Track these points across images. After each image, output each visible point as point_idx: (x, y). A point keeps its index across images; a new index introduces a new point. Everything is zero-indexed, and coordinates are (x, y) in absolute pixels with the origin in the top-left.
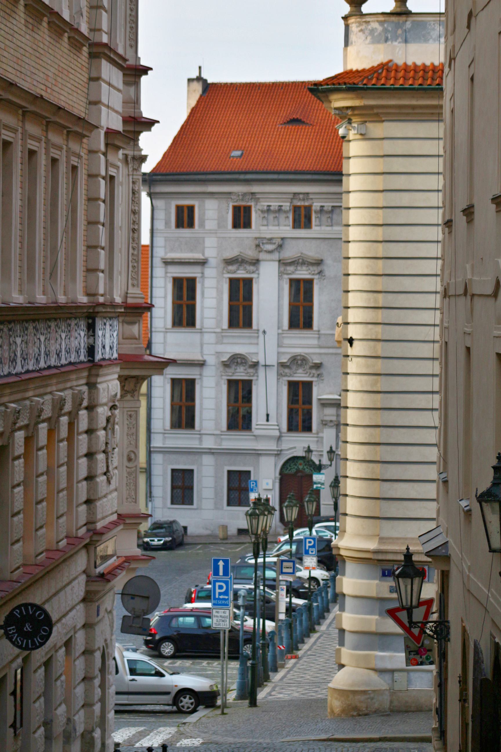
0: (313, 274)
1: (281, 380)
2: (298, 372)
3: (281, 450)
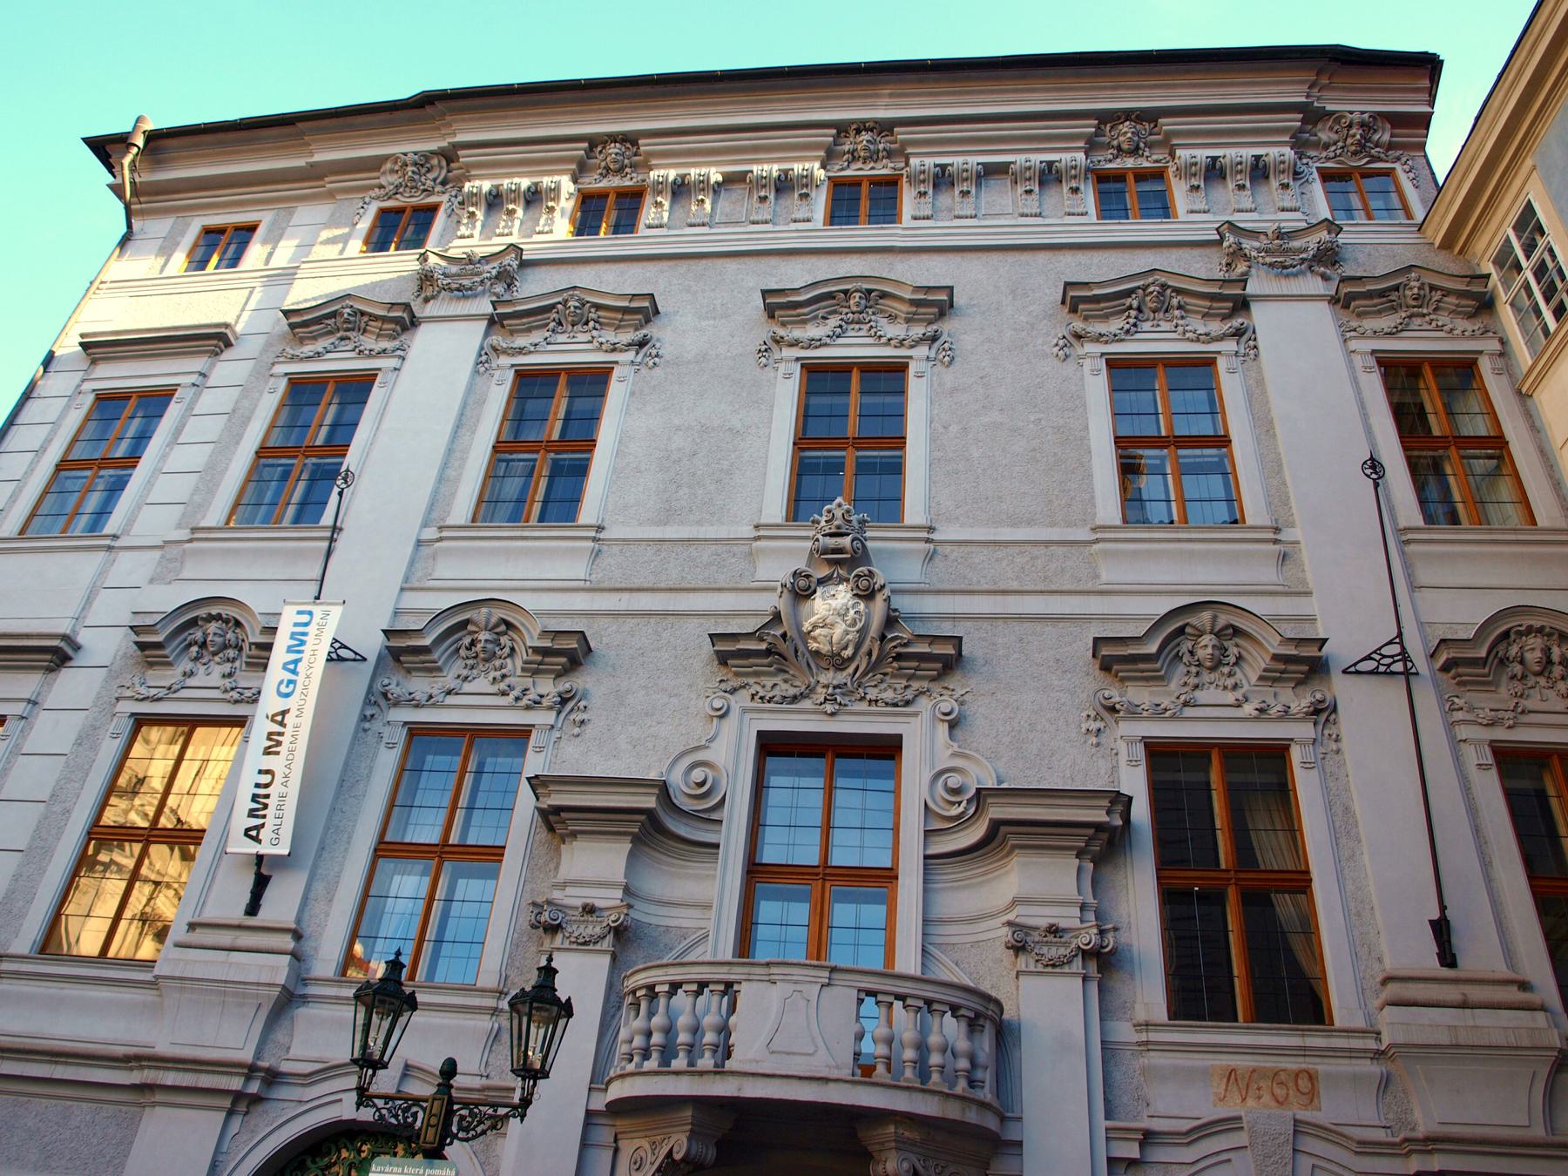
0: (614, 349)
1: (376, 726)
2: (467, 687)
3: (273, 1077)
